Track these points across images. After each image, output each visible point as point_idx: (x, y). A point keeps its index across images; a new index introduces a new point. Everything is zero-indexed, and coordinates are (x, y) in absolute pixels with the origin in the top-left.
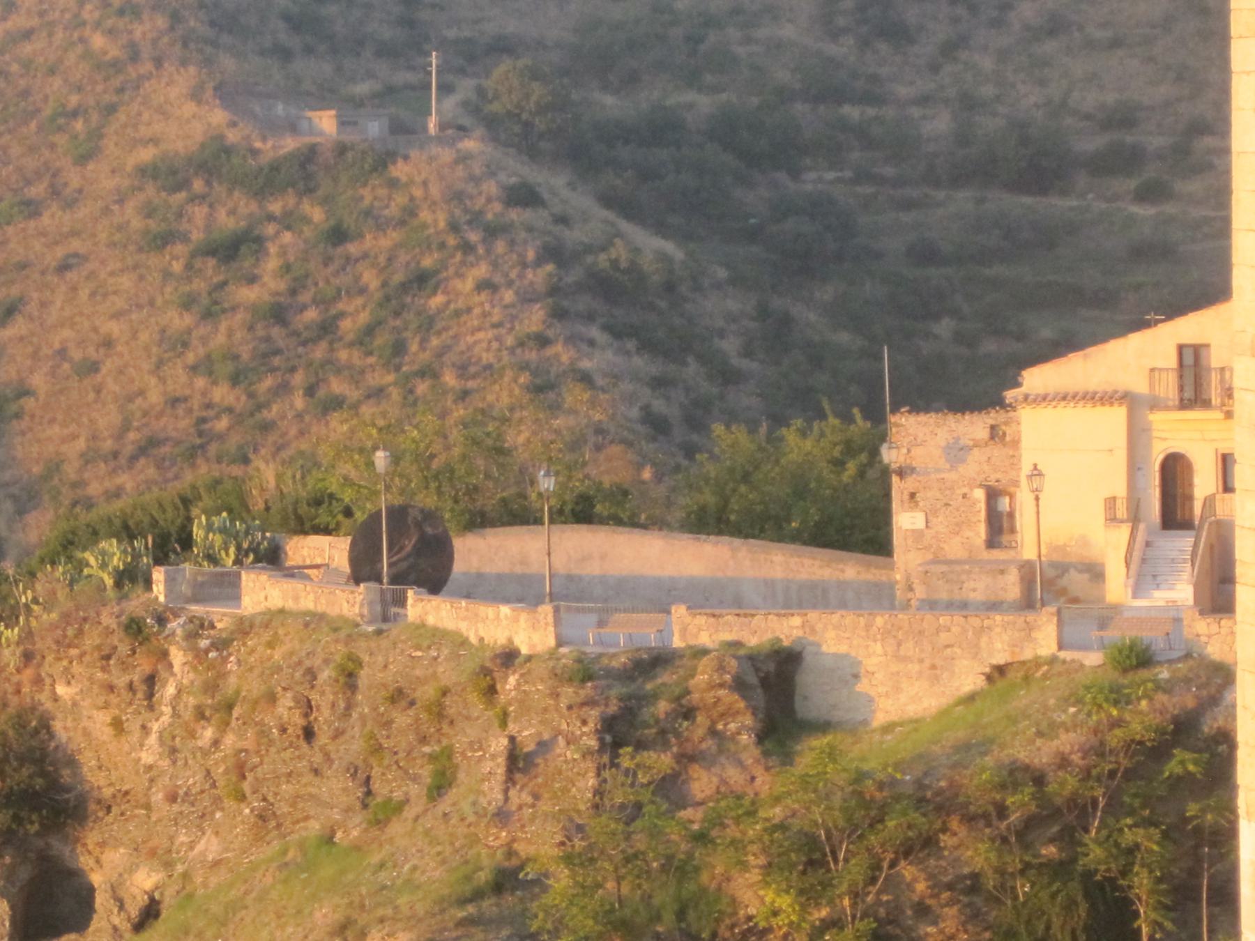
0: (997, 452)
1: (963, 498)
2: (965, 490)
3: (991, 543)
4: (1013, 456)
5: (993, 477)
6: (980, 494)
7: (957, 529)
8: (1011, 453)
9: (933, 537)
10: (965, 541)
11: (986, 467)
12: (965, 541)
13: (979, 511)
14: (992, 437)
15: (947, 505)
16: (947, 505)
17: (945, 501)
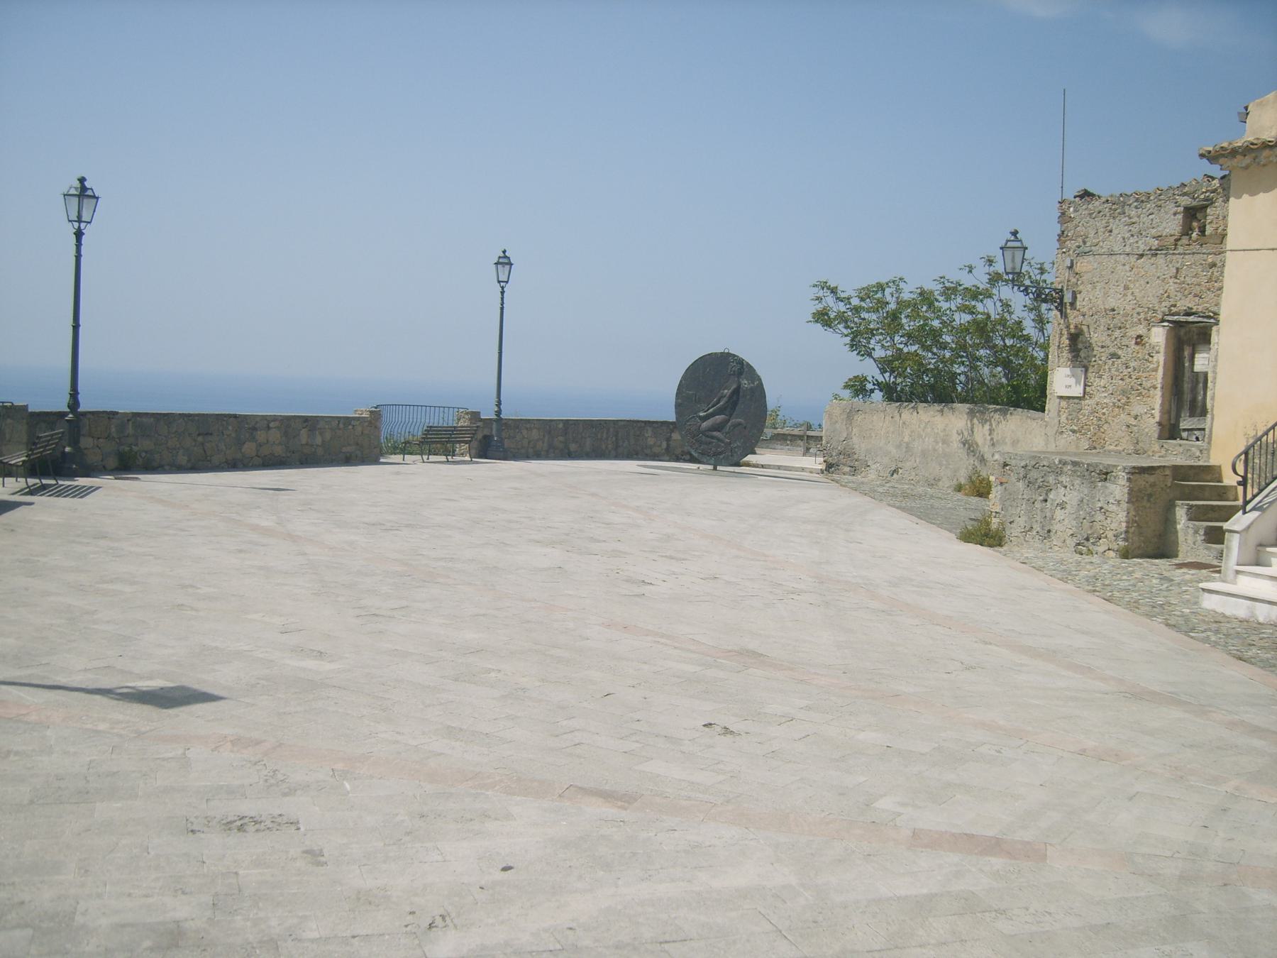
0: (1191, 261)
1: (1137, 343)
2: (1141, 330)
3: (1170, 431)
4: (1213, 265)
5: (1183, 305)
6: (1158, 336)
7: (1125, 397)
8: (1210, 259)
9: (1094, 412)
10: (1133, 422)
11: (1172, 287)
12: (1133, 422)
13: (1156, 370)
14: (1187, 231)
15: (1114, 356)
16: (1114, 356)
17: (1112, 350)
